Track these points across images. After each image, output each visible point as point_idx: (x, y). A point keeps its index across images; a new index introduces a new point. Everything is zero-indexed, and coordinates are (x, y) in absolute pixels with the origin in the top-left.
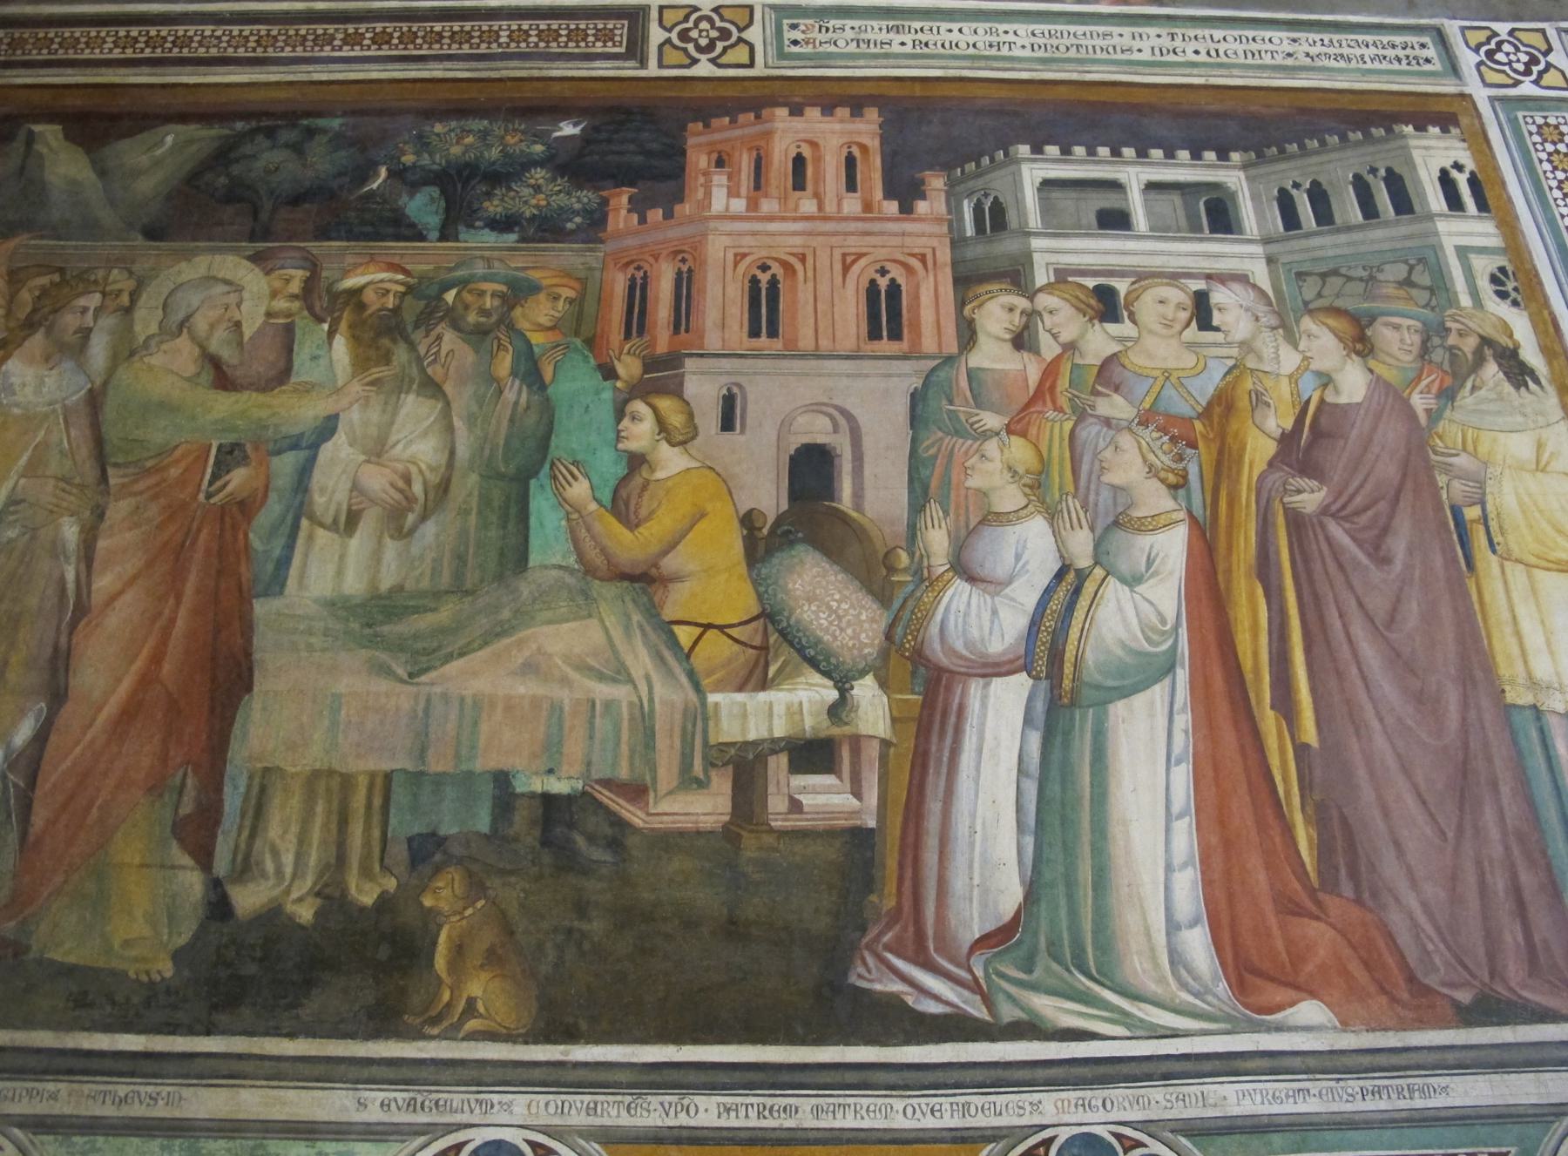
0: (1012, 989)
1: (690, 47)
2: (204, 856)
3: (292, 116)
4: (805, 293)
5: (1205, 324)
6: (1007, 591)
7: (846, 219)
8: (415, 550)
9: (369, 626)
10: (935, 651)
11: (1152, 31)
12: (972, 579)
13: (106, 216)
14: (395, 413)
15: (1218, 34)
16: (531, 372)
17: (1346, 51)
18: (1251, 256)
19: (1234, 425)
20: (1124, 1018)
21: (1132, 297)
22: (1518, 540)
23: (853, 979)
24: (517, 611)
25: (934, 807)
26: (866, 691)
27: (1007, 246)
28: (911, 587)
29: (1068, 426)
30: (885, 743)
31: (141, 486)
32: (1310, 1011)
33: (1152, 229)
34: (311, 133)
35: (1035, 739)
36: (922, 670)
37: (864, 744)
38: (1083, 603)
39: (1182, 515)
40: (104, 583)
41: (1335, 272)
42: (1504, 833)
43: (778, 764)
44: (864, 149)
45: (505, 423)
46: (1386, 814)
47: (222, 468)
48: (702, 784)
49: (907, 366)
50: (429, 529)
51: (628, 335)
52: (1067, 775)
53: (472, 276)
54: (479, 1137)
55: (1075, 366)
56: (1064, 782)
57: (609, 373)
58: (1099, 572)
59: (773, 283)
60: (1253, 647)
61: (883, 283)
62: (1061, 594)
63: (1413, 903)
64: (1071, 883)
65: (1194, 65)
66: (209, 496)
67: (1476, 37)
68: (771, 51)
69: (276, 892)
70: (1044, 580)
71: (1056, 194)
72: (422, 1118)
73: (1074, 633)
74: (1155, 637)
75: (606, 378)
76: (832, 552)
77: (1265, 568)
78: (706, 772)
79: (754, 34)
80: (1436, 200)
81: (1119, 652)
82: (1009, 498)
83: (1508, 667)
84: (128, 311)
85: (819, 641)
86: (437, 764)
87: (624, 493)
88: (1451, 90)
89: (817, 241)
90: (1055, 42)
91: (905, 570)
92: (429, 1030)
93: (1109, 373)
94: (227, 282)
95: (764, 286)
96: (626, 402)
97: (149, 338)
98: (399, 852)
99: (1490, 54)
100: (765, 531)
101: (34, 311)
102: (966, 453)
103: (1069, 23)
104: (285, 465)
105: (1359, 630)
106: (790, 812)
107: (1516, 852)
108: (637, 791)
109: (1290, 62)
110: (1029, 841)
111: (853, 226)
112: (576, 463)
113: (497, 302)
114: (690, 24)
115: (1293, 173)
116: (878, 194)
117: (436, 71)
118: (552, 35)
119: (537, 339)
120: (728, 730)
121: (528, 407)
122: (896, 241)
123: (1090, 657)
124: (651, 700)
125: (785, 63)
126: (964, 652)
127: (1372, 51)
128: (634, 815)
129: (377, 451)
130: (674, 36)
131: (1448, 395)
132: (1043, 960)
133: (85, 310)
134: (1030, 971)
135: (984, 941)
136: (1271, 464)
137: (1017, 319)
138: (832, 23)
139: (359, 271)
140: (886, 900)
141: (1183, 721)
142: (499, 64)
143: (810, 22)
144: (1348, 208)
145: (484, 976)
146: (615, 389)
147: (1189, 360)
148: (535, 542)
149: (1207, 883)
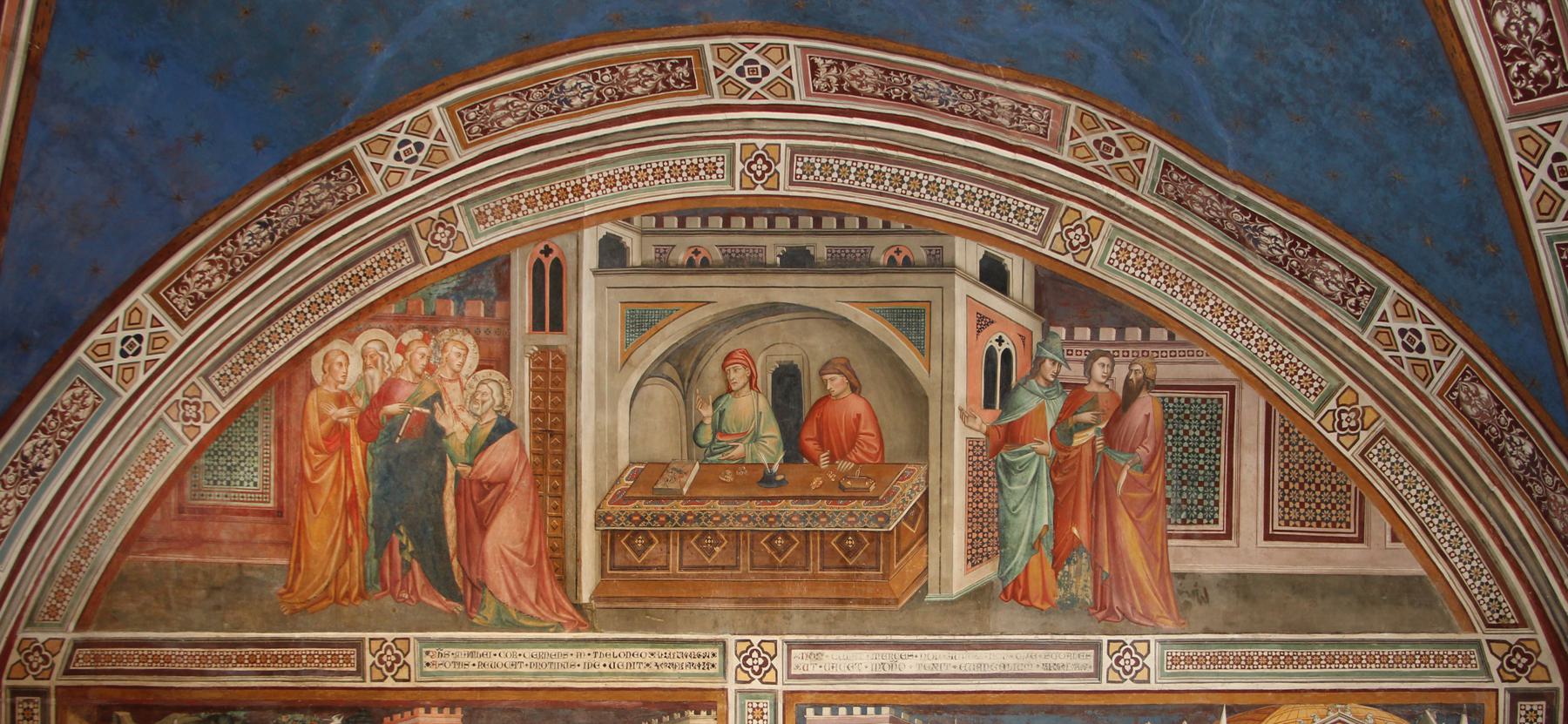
11: (586, 651)
15: (617, 651)
17: (676, 661)
65: (601, 674)
67: (743, 646)
68: (418, 672)
79: (410, 659)
90: (541, 661)
99: (746, 659)
103: (550, 647)
109: (647, 670)
114: (382, 652)
118: (323, 658)
130: (376, 659)
138: (445, 650)
142: (305, 678)
143: (434, 650)
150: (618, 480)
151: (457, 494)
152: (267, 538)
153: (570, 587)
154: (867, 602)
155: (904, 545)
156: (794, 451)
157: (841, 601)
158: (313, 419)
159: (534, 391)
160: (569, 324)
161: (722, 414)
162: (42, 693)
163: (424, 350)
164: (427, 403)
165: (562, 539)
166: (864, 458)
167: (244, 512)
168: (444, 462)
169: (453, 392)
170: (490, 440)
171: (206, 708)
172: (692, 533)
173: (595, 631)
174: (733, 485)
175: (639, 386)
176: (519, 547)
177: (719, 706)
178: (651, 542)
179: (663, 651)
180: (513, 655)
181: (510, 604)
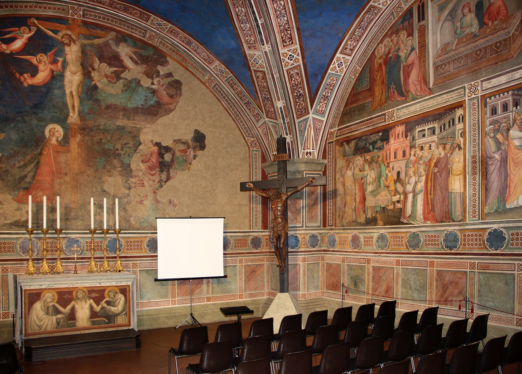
3: (361, 137)
5: (430, 149)
15: (438, 98)
20: (417, 223)
22: (454, 172)
26: (402, 195)
27: (415, 142)
32: (429, 222)
40: (357, 192)
52: (414, 203)
57: (385, 166)
60: (429, 188)
67: (469, 86)
76: (399, 182)
79: (394, 115)
82: (412, 175)
83: (450, 188)
88: (463, 99)
93: (421, 158)
108: (388, 206)
115: (442, 122)
127: (455, 95)
131: (452, 154)
138: (401, 110)
141: (423, 196)
150: (438, 52)
151: (403, 70)
152: (368, 95)
153: (428, 84)
154: (504, 61)
155: (515, 39)
156: (482, 24)
157: (496, 63)
158: (376, 64)
159: (418, 38)
160: (426, 17)
161: (462, 23)
163: (396, 39)
164: (397, 51)
165: (425, 73)
166: (503, 18)
167: (364, 91)
168: (400, 64)
169: (402, 46)
170: (410, 54)
171: (358, 138)
172: (456, 59)
173: (433, 94)
174: (466, 41)
175: (442, 25)
176: (416, 79)
177: (464, 105)
178: (446, 65)
179: (449, 94)
180: (416, 107)
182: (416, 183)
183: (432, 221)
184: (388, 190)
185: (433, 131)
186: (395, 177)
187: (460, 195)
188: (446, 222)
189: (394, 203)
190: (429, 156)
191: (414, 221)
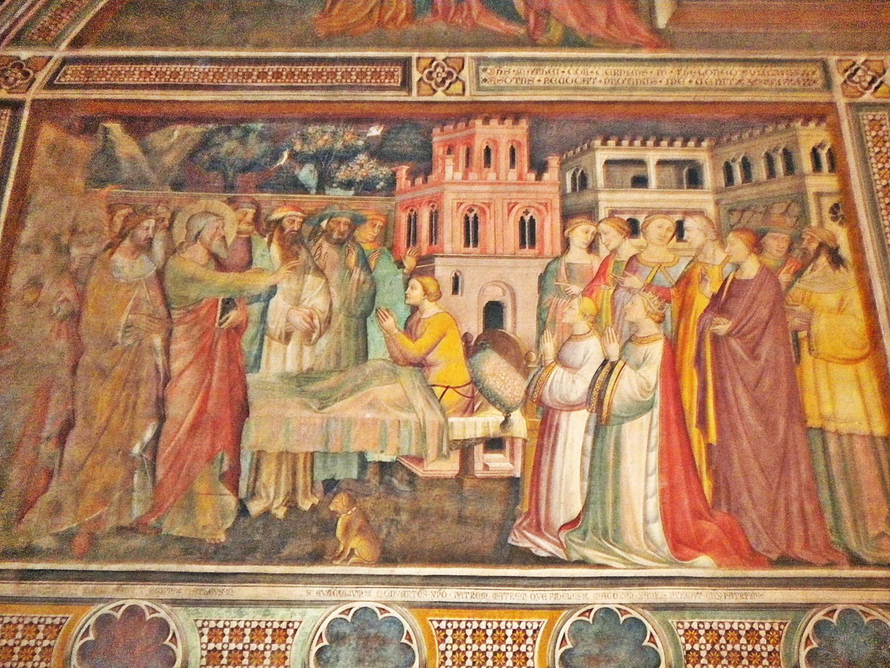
0: (576, 547)
1: (433, 83)
2: (235, 489)
3: (238, 122)
4: (490, 226)
6: (579, 372)
7: (510, 184)
8: (317, 352)
9: (299, 386)
10: (547, 399)
11: (669, 68)
12: (565, 366)
13: (153, 177)
14: (303, 285)
16: (365, 263)
18: (706, 201)
19: (690, 291)
21: (646, 223)
22: (825, 347)
23: (510, 541)
24: (364, 380)
25: (545, 468)
26: (517, 416)
27: (587, 198)
28: (536, 370)
29: (611, 292)
30: (525, 441)
31: (188, 319)
33: (658, 187)
34: (247, 132)
35: (590, 439)
36: (541, 409)
37: (515, 441)
38: (613, 377)
39: (662, 336)
40: (176, 366)
41: (748, 208)
42: (800, 485)
43: (479, 449)
44: (519, 144)
45: (354, 290)
46: (746, 475)
47: (225, 311)
48: (446, 457)
49: (536, 262)
50: (323, 342)
51: (408, 245)
52: (603, 458)
53: (334, 213)
54: (357, 606)
55: (616, 262)
56: (601, 458)
57: (400, 264)
58: (621, 364)
59: (476, 218)
60: (690, 399)
61: (527, 218)
62: (604, 373)
63: (753, 515)
64: (603, 503)
66: (220, 324)
69: (267, 505)
70: (596, 367)
71: (612, 168)
72: (334, 598)
73: (608, 392)
74: (644, 394)
75: (399, 268)
77: (699, 360)
78: (448, 453)
79: (465, 74)
80: (807, 164)
81: (628, 401)
82: (582, 326)
84: (169, 228)
85: (496, 394)
86: (333, 447)
87: (409, 324)
89: (494, 196)
91: (534, 362)
92: (334, 562)
93: (632, 264)
94: (217, 215)
95: (471, 220)
96: (409, 280)
97: (182, 243)
98: (319, 487)
100: (473, 343)
101: (123, 228)
102: (563, 306)
104: (256, 308)
105: (740, 390)
106: (484, 469)
107: (804, 495)
108: (419, 460)
110: (586, 484)
111: (512, 188)
112: (388, 310)
113: (347, 228)
115: (733, 153)
116: (526, 169)
117: (306, 96)
118: (362, 75)
119: (367, 247)
120: (458, 434)
121: (364, 283)
122: (533, 196)
123: (616, 403)
124: (424, 421)
125: (480, 93)
126: (559, 400)
128: (418, 470)
129: (297, 302)
131: (798, 274)
132: (590, 535)
133: (148, 229)
134: (584, 540)
135: (565, 526)
136: (705, 311)
137: (590, 237)
138: (505, 68)
139: (280, 209)
140: (524, 507)
141: (656, 432)
144: (760, 171)
145: (357, 539)
146: (403, 273)
147: (670, 257)
148: (371, 348)
149: (663, 503)
162: (17, 106)
181: (578, 28)
182: (607, 366)
183: (724, 553)
184: (425, 379)
185: (694, 179)
186: (475, 326)
187: (875, 447)
188: (809, 564)
189: (465, 449)
190: (676, 262)
191: (607, 551)
